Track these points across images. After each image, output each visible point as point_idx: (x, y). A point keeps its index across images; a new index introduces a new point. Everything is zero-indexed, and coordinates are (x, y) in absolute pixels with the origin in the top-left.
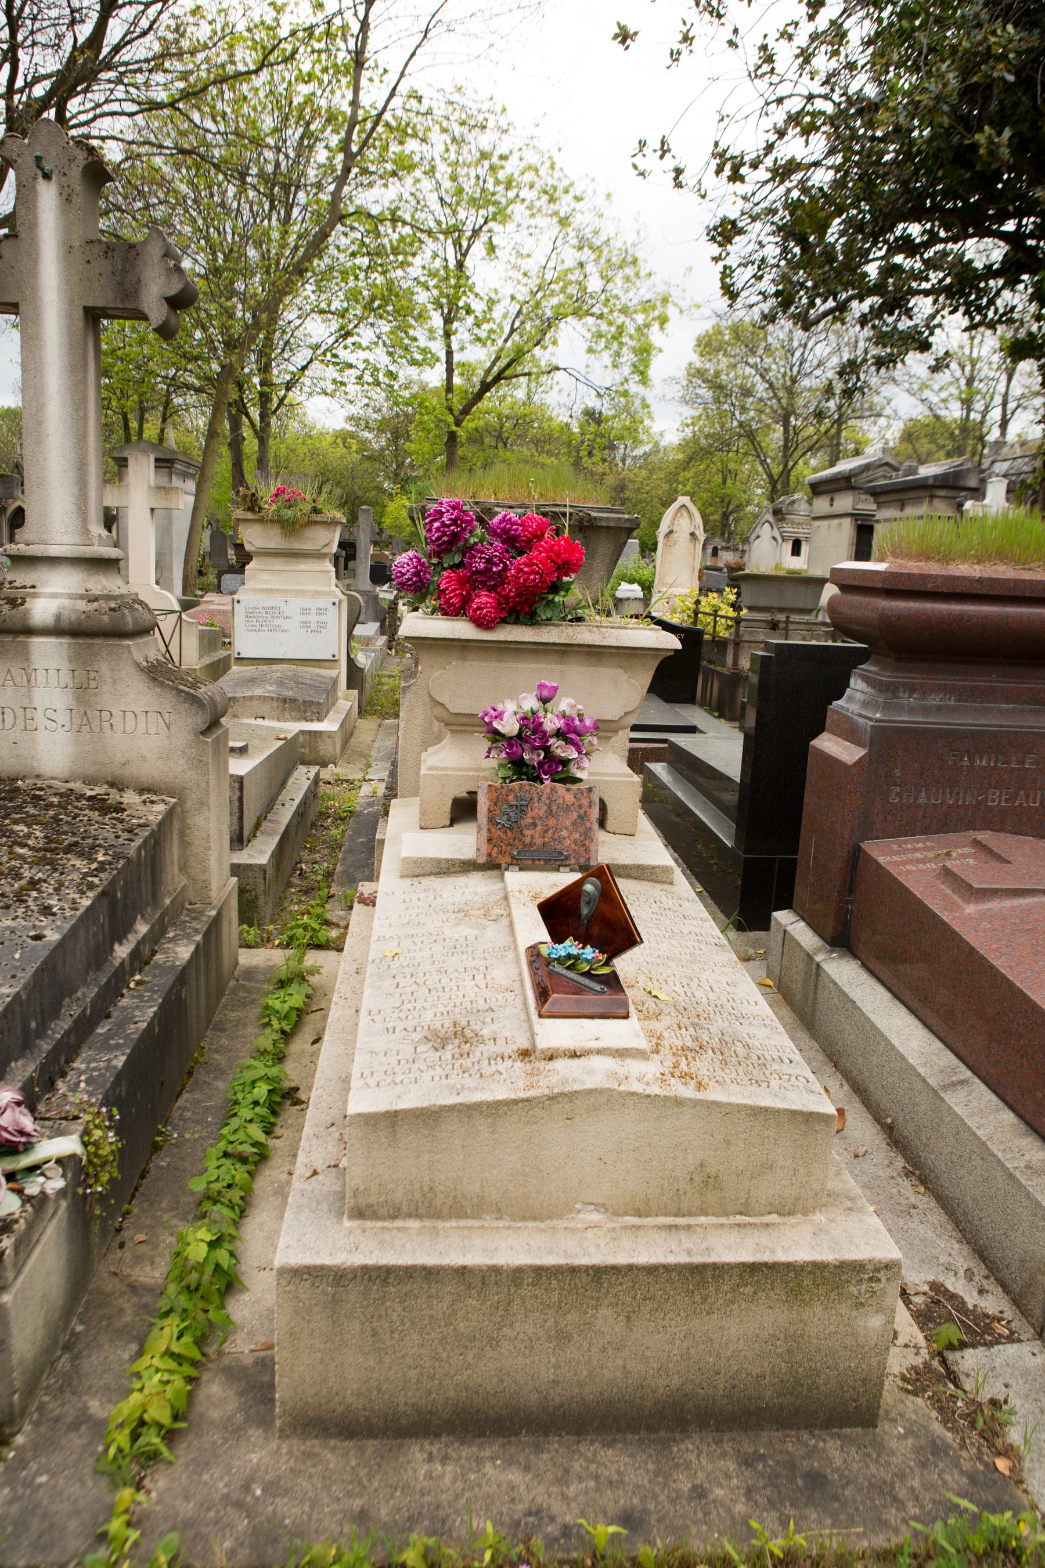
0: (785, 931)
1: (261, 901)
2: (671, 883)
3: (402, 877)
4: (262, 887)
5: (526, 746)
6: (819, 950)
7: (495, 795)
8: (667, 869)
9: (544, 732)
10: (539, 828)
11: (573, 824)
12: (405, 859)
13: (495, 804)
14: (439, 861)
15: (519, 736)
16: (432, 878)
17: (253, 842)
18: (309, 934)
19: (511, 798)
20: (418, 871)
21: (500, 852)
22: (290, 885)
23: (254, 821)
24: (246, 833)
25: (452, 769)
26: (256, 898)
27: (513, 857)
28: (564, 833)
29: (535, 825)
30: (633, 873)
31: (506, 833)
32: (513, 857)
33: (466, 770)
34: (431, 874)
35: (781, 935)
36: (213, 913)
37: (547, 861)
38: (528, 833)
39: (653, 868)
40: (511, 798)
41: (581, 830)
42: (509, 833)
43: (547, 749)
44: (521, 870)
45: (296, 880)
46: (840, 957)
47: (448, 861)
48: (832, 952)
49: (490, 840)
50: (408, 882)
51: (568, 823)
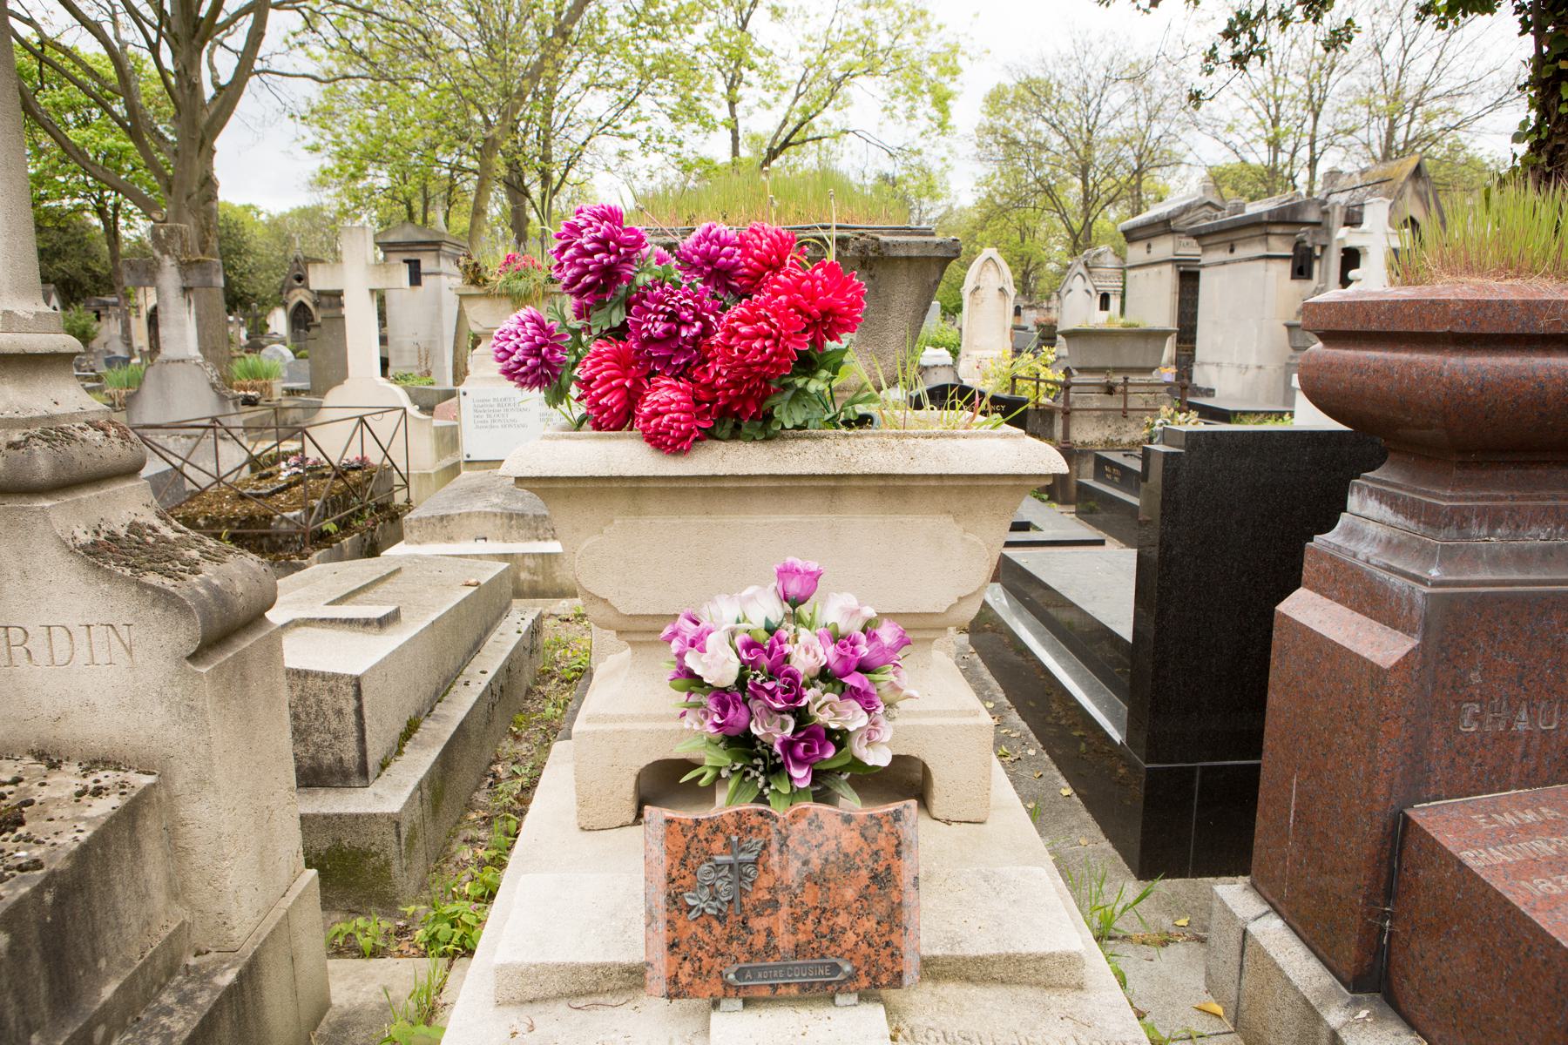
0: (1245, 932)
1: (395, 868)
2: (1080, 987)
3: (498, 1004)
4: (395, 848)
5: (756, 706)
6: (1328, 995)
7: (681, 841)
8: (1070, 961)
9: (793, 676)
10: (784, 911)
11: (863, 897)
12: (504, 966)
13: (683, 863)
14: (576, 970)
15: (741, 681)
16: (561, 1008)
17: (394, 767)
18: (459, 932)
19: (717, 845)
20: (531, 992)
21: (697, 973)
22: (470, 806)
23: (401, 727)
24: (373, 759)
25: (633, 718)
26: (388, 863)
27: (727, 985)
28: (842, 920)
29: (774, 904)
30: (997, 971)
32: (727, 985)
33: (659, 718)
34: (560, 996)
35: (1235, 936)
36: (227, 978)
37: (803, 987)
38: (758, 924)
39: (1041, 958)
40: (717, 845)
41: (881, 908)
43: (802, 716)
44: (747, 1003)
45: (481, 797)
46: (1378, 1017)
47: (594, 968)
48: (1357, 1003)
49: (673, 946)
50: (515, 1018)
51: (850, 894)
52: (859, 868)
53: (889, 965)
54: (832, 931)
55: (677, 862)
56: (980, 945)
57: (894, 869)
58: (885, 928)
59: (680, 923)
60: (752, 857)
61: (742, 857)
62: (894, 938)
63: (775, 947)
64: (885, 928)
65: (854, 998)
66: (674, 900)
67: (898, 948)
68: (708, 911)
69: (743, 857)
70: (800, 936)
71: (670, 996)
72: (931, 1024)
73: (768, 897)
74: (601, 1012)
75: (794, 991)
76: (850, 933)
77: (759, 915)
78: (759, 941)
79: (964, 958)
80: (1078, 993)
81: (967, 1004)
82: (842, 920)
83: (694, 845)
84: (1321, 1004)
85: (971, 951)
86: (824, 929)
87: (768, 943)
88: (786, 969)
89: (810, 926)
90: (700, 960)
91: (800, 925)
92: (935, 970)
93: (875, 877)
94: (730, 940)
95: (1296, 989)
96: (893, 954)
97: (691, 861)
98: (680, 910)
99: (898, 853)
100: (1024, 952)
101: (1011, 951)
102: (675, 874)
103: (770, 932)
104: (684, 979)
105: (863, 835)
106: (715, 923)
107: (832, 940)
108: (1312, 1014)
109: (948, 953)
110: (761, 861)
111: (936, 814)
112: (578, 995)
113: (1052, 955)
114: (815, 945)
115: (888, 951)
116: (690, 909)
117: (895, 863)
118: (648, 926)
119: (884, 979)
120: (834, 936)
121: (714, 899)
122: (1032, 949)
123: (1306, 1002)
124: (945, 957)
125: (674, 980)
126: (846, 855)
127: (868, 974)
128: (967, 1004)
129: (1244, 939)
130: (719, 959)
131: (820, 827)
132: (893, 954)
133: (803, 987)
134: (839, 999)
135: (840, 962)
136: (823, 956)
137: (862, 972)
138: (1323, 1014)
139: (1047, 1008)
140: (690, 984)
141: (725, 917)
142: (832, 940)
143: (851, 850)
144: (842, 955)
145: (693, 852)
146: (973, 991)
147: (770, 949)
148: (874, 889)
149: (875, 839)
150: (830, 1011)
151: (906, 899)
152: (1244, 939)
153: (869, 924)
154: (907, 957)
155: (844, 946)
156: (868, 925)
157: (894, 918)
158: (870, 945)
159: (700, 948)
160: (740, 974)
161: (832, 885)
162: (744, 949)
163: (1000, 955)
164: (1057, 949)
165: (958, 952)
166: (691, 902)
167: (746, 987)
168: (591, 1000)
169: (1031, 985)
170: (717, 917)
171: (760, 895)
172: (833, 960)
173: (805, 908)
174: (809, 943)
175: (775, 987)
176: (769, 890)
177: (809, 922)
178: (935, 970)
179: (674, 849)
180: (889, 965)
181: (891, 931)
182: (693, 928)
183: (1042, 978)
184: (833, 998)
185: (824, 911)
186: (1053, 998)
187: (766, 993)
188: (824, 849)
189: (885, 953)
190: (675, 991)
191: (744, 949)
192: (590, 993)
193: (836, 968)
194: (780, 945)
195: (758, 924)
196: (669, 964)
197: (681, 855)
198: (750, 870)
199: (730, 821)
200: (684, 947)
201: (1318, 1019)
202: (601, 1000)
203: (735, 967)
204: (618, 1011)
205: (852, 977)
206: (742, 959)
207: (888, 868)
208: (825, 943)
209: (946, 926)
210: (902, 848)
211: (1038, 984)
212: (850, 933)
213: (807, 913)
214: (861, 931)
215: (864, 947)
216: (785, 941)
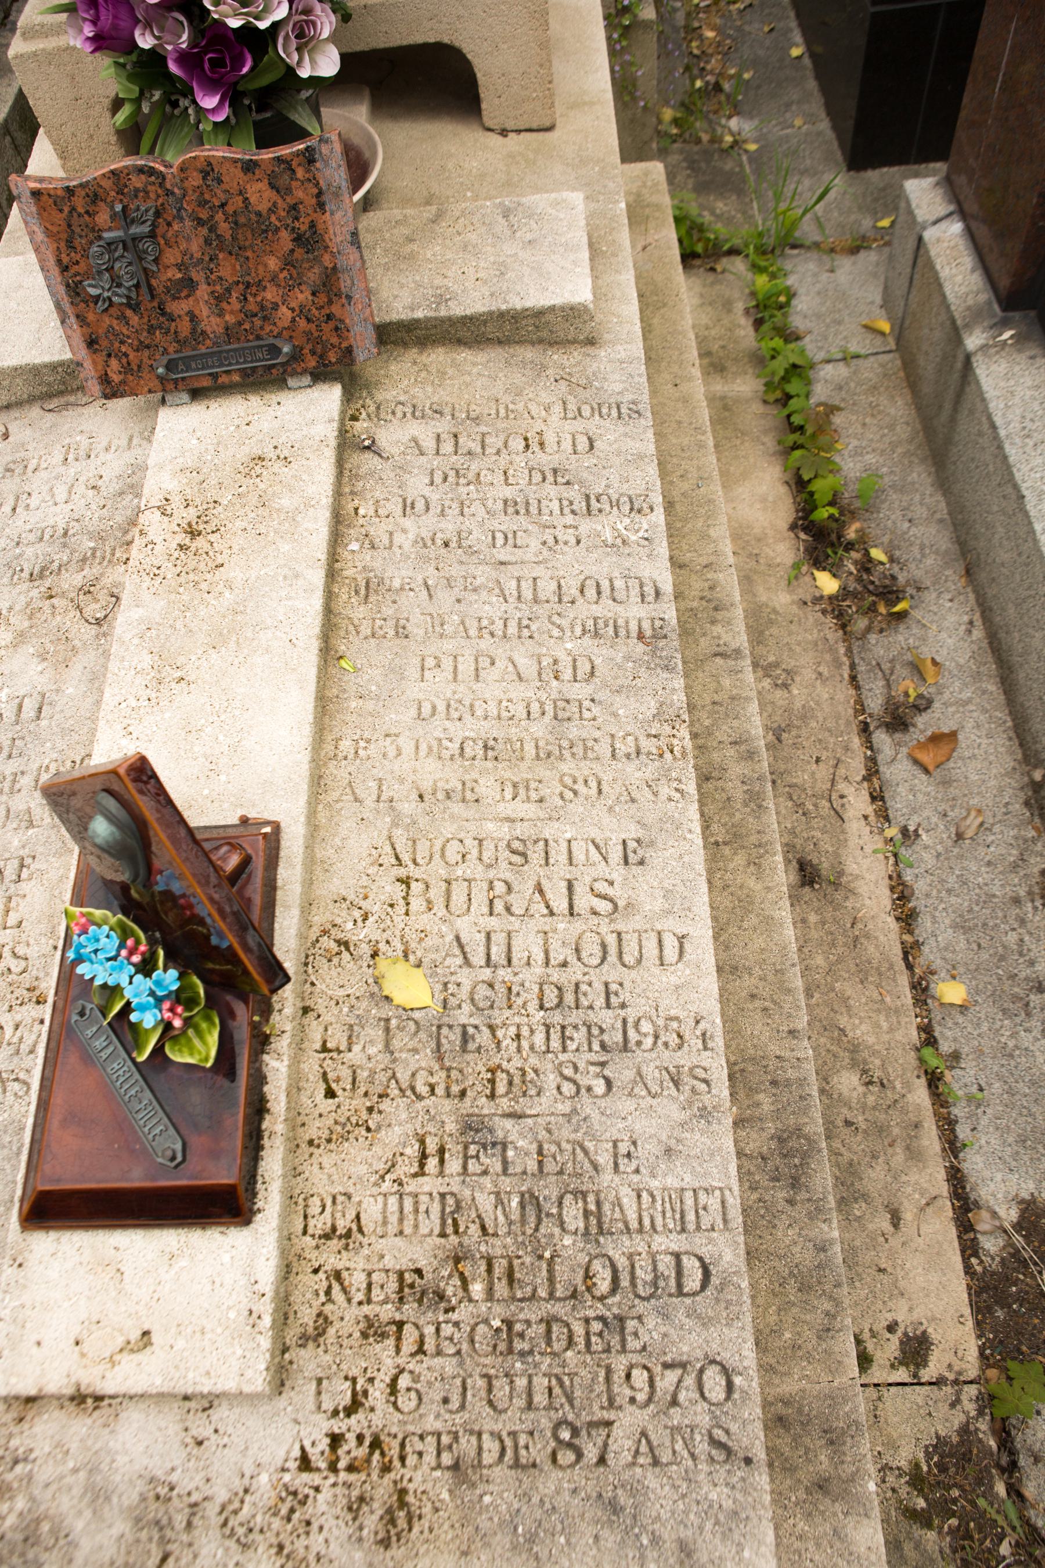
0: (920, 239)
2: (591, 342)
6: (976, 315)
7: (59, 218)
10: (203, 291)
11: (288, 263)
13: (70, 245)
14: (35, 371)
16: (35, 412)
19: (103, 218)
28: (270, 294)
29: (190, 284)
30: (490, 330)
31: (122, 318)
34: (32, 400)
35: (911, 244)
37: (244, 373)
38: (179, 307)
39: (539, 313)
40: (103, 218)
41: (313, 275)
42: (135, 320)
44: (196, 394)
46: (1020, 340)
48: (1004, 324)
51: (273, 263)
52: (277, 230)
53: (334, 340)
54: (262, 308)
55: (63, 244)
56: (472, 301)
57: (320, 226)
58: (322, 299)
59: (91, 317)
60: (146, 229)
61: (135, 230)
62: (335, 309)
63: (203, 332)
64: (322, 299)
65: (307, 380)
66: (74, 290)
67: (342, 321)
68: (115, 299)
69: (135, 230)
70: (227, 318)
71: (106, 397)
72: (402, 398)
73: (179, 276)
74: (70, 413)
75: (236, 378)
76: (284, 309)
77: (175, 298)
78: (184, 327)
79: (450, 319)
80: (590, 350)
81: (450, 372)
82: (270, 294)
83: (75, 220)
84: (966, 326)
85: (457, 310)
86: (252, 307)
87: (194, 330)
88: (220, 356)
89: (236, 306)
90: (126, 355)
91: (224, 305)
92: (395, 336)
93: (298, 239)
94: (151, 330)
95: (948, 307)
96: (337, 329)
97: (78, 242)
98: (86, 302)
99: (321, 206)
100: (518, 307)
101: (504, 307)
102: (66, 260)
103: (193, 317)
104: (116, 378)
105: (272, 186)
106: (129, 313)
107: (265, 318)
108: (955, 335)
109: (431, 314)
110: (160, 231)
111: (489, 123)
112: (50, 396)
113: (552, 308)
114: (247, 326)
115: (331, 324)
116: (96, 299)
117: (320, 219)
118: (63, 322)
119: (332, 357)
120: (267, 313)
121: (119, 285)
122: (529, 304)
123: (953, 321)
124: (428, 319)
125: (105, 380)
126: (259, 214)
127: (313, 353)
128: (450, 372)
129: (918, 248)
130: (146, 353)
131: (220, 181)
132: (337, 329)
133: (244, 373)
134: (291, 382)
135: (278, 342)
136: (258, 338)
137: (306, 351)
138: (965, 336)
139: (544, 368)
140: (123, 382)
141: (138, 304)
142: (265, 318)
143: (263, 207)
144: (279, 336)
145: (78, 230)
146: (464, 355)
147: (198, 335)
148: (300, 253)
149: (289, 190)
150: (284, 396)
151: (341, 262)
152: (918, 248)
153: (302, 296)
154: (357, 329)
155: (280, 324)
156: (301, 297)
157: (330, 287)
158: (309, 320)
159: (122, 342)
160: (170, 366)
161: (249, 254)
162: (170, 338)
163: (491, 313)
164: (557, 301)
165: (443, 313)
166: (93, 291)
167: (183, 379)
168: (62, 400)
169: (533, 344)
170: (129, 305)
171: (169, 275)
172: (271, 341)
173: (226, 285)
174: (240, 324)
175: (215, 376)
176: (179, 267)
177: (233, 299)
178: (395, 336)
179: (55, 229)
180: (334, 340)
181: (330, 302)
182: (107, 320)
183: (544, 334)
184: (285, 381)
185: (248, 285)
186: (556, 356)
187: (206, 383)
188: (230, 209)
189: (327, 328)
190: (111, 391)
191: (170, 338)
192: (61, 393)
193: (275, 350)
194: (209, 330)
195: (179, 307)
196: (94, 363)
197: (64, 236)
198: (147, 245)
199: (107, 184)
200: (104, 343)
201: (959, 341)
202: (72, 399)
203: (165, 360)
204: (86, 411)
205: (296, 356)
206: (171, 350)
207: (313, 225)
208: (258, 323)
209: (438, 281)
210: (326, 198)
211: (541, 341)
212: (284, 309)
213: (228, 290)
214: (293, 305)
215: (302, 323)
216: (212, 324)
